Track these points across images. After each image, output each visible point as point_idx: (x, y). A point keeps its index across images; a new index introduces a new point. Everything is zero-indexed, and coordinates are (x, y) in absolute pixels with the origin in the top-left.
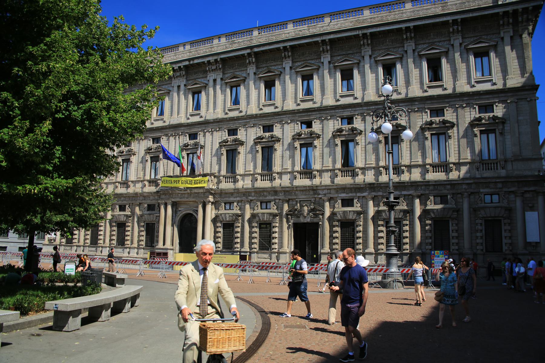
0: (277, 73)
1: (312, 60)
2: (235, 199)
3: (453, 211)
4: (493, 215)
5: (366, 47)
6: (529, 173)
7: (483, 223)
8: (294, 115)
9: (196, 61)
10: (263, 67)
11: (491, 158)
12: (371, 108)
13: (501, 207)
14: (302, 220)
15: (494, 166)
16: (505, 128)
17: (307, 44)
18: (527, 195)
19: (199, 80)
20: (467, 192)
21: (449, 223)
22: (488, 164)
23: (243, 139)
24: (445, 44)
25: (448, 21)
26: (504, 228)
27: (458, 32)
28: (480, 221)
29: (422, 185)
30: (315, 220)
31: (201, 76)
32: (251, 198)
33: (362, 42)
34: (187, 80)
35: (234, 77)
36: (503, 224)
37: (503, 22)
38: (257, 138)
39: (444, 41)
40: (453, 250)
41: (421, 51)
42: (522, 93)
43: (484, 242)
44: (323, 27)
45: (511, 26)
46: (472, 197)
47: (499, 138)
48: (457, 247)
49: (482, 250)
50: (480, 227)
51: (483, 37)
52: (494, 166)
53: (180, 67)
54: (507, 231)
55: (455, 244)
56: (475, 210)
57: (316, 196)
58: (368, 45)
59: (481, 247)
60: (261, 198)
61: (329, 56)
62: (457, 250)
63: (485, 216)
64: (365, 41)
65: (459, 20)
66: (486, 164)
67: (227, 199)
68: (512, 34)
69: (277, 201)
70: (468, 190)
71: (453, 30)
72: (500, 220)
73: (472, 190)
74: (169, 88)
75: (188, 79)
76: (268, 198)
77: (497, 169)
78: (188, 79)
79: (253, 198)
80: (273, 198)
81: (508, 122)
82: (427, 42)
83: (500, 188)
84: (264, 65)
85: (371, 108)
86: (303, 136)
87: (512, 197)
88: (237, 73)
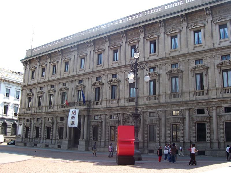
2: (99, 114)
4: (229, 120)
12: (164, 61)
17: (133, 29)
20: (215, 106)
21: (205, 125)
22: (227, 89)
23: (104, 82)
24: (203, 21)
27: (209, 14)
32: (106, 113)
35: (99, 50)
38: (109, 81)
40: (207, 140)
41: (190, 27)
46: (218, 109)
50: (222, 127)
51: (224, 16)
58: (163, 26)
60: (111, 113)
63: (225, 120)
65: (209, 8)
67: (95, 114)
69: (119, 114)
70: (215, 105)
71: (207, 13)
73: (217, 105)
76: (114, 113)
79: (107, 113)
82: (194, 21)
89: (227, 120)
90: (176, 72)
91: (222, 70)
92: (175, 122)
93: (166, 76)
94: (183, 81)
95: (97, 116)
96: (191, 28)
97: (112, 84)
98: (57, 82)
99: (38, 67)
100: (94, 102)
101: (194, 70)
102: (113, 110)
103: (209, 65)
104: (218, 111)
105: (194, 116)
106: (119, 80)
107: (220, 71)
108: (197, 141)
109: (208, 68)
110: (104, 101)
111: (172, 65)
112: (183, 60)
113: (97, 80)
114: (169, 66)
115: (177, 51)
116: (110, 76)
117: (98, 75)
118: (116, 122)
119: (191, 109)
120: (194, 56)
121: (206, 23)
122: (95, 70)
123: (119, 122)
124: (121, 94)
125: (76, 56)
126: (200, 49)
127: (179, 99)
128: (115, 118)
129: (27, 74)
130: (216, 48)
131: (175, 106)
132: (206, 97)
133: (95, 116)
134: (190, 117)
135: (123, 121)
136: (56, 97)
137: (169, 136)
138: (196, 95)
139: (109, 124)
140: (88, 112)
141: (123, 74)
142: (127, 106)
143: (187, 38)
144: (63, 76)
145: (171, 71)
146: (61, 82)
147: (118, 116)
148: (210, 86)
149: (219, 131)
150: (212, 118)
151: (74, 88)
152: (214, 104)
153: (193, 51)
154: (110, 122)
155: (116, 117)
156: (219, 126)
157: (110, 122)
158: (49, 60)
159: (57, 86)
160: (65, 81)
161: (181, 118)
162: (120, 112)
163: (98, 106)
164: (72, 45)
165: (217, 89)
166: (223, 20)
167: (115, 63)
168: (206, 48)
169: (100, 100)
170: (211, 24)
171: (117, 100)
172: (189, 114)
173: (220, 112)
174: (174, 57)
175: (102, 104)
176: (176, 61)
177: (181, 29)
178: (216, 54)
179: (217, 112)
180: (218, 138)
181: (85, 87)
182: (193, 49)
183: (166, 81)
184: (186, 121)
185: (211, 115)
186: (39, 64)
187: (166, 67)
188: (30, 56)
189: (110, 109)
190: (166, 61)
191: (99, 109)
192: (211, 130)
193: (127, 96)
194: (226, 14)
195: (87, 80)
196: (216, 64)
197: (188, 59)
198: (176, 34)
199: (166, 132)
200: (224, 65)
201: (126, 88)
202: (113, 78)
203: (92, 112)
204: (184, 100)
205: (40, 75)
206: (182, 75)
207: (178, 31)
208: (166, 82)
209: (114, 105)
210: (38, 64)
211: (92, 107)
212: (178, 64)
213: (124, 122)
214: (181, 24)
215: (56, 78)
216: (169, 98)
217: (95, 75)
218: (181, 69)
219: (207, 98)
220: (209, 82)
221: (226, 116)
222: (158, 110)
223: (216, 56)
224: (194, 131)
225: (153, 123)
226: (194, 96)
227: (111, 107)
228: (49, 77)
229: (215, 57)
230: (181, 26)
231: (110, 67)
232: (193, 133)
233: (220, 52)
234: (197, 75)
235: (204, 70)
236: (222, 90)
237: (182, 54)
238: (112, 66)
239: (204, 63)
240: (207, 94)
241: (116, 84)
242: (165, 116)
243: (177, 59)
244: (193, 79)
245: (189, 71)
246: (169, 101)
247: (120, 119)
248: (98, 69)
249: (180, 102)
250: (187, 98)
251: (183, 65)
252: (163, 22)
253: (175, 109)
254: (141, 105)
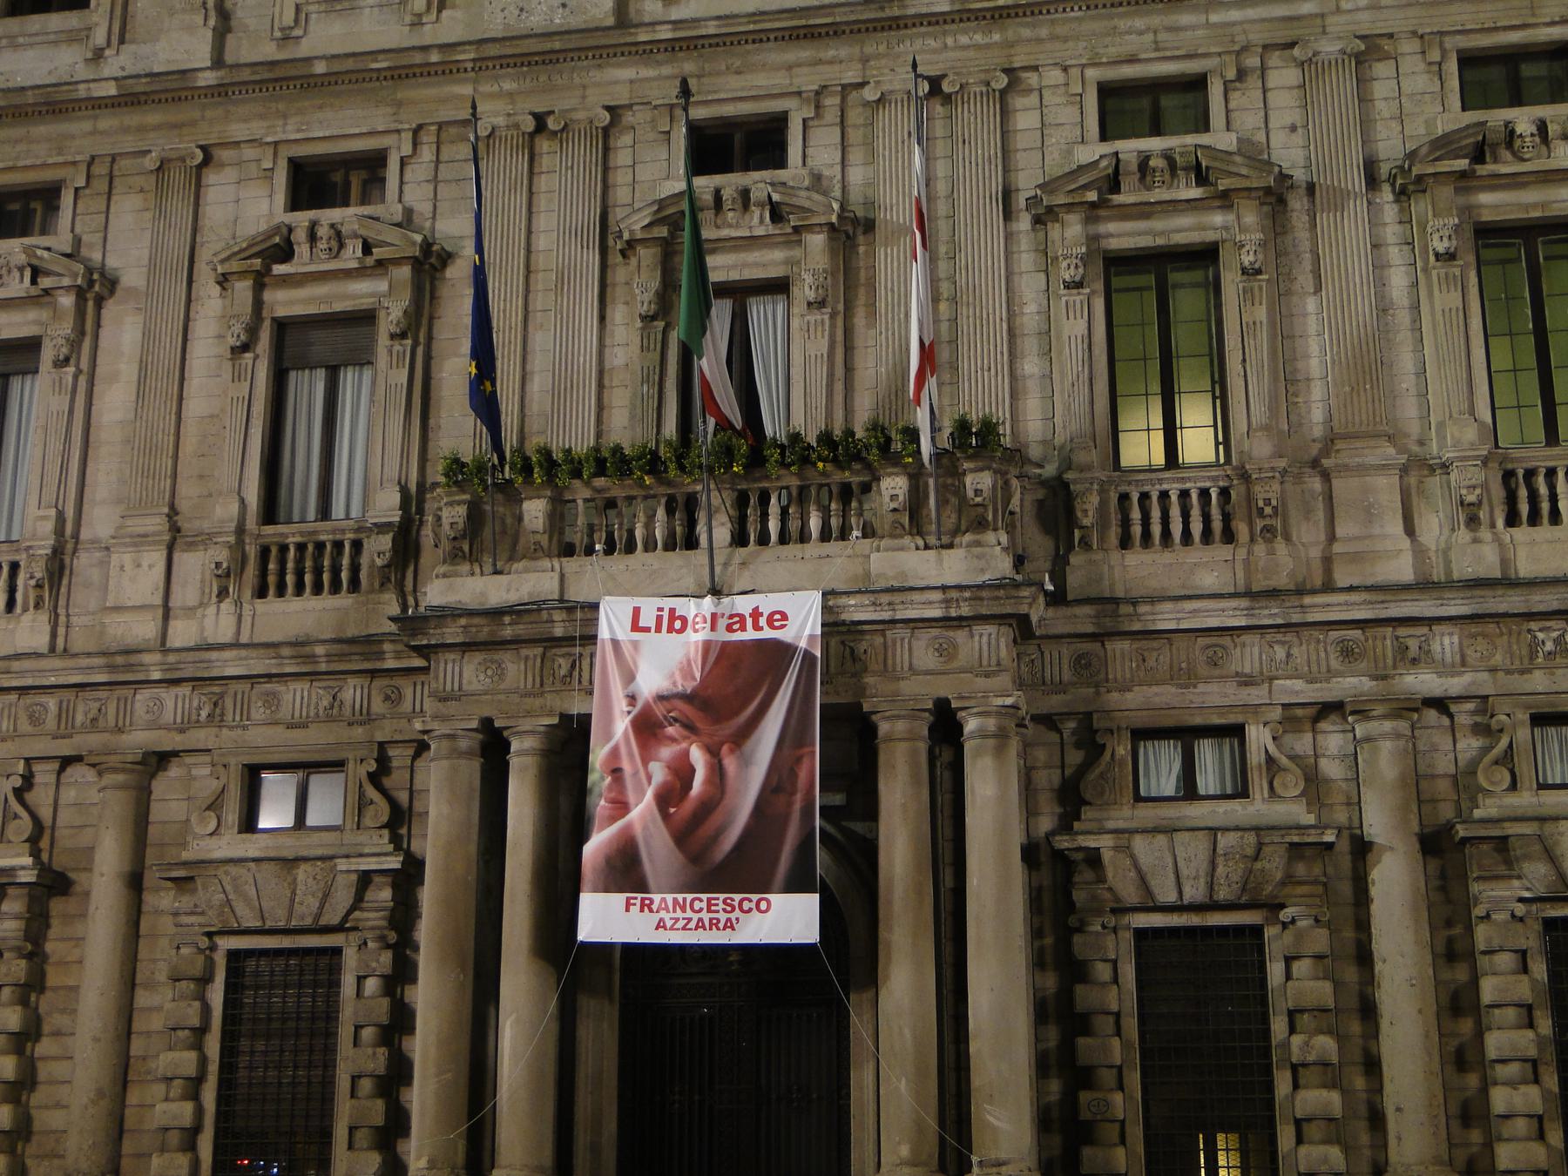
32: (1422, 682)
60: (1538, 681)
79: (1454, 685)
98: (157, 136)
146: (238, 131)
159: (129, 212)
191: (1270, 614)
217: (1075, 52)
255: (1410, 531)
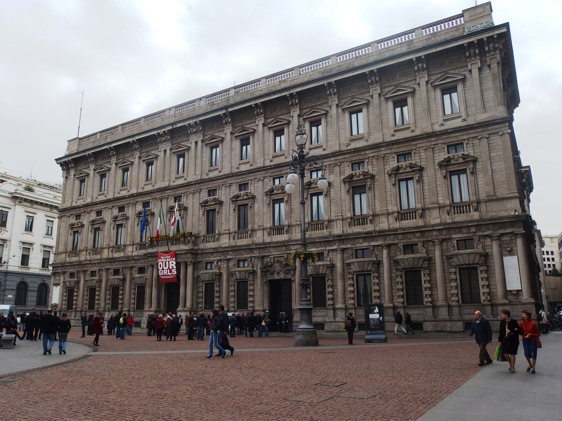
0: (251, 131)
1: (283, 115)
2: (215, 259)
3: (424, 260)
4: (467, 262)
5: (332, 96)
6: (505, 214)
7: (458, 272)
8: (267, 172)
9: (178, 125)
10: (239, 126)
11: (464, 200)
12: (339, 158)
13: (475, 254)
14: (276, 277)
15: (466, 209)
16: (477, 167)
18: (505, 238)
19: (183, 143)
23: (223, 199)
24: (412, 84)
25: (412, 59)
26: (480, 276)
27: (423, 69)
28: (454, 270)
29: (390, 235)
30: (289, 277)
31: (184, 139)
32: (229, 257)
33: (328, 92)
34: (172, 144)
36: (479, 272)
37: (470, 54)
38: (233, 197)
39: (410, 81)
41: (386, 94)
42: (493, 127)
43: (460, 293)
44: (293, 80)
45: (478, 57)
46: (444, 244)
47: (471, 178)
48: (430, 299)
49: (458, 301)
50: (453, 277)
52: (466, 209)
53: (164, 132)
54: (484, 279)
55: (428, 296)
56: (449, 258)
57: (288, 252)
58: (335, 94)
59: (456, 298)
60: (238, 256)
61: (298, 109)
62: (431, 302)
64: (331, 90)
66: (457, 207)
67: (208, 259)
68: (479, 66)
69: (253, 259)
71: (418, 68)
72: (477, 267)
73: (443, 237)
74: (157, 153)
75: (173, 143)
76: (244, 256)
77: (470, 212)
78: (173, 143)
79: (231, 257)
80: (248, 256)
81: (480, 160)
83: (473, 233)
84: (240, 124)
85: (339, 158)
86: (275, 191)
87: (488, 241)
88: (216, 134)
89: (462, 263)
90: (361, 177)
91: (450, 172)
92: (362, 269)
93: (343, 185)
94: (374, 194)
95: (212, 263)
96: (388, 96)
97: (239, 203)
98: (132, 201)
99: (91, 173)
100: (204, 236)
101: (395, 172)
102: (242, 252)
103: (423, 164)
104: (444, 247)
105: (399, 257)
106: (253, 196)
107: (446, 173)
108: (406, 304)
109: (423, 168)
110: (226, 234)
111: (352, 164)
112: (374, 154)
113: (209, 195)
114: (348, 168)
115: (361, 138)
116: (235, 188)
117: (211, 185)
118: (250, 273)
119: (393, 244)
120: (396, 146)
121: (416, 87)
122: (206, 177)
123: (254, 273)
124: (256, 220)
125: (168, 151)
126: (407, 134)
127: (369, 227)
128: (246, 265)
129: (69, 186)
130: (437, 132)
131: (361, 241)
132: (420, 222)
133: (207, 263)
134: (390, 260)
135: (262, 272)
136: (129, 229)
137: (352, 295)
138: (400, 218)
139: (235, 276)
140: (194, 256)
141: (260, 183)
142: (269, 243)
143: (381, 114)
144: (143, 188)
145: (351, 177)
146: (138, 200)
147: (252, 262)
148: (427, 200)
149: (448, 285)
150: (433, 261)
151: (165, 212)
152: (436, 235)
153: (393, 139)
154: (237, 273)
155: (249, 264)
156: (446, 275)
157: (237, 273)
158: (114, 160)
159: (130, 208)
160: (146, 198)
161: (374, 263)
162: (256, 254)
163: (212, 245)
164: (159, 131)
165: (440, 207)
166: (450, 80)
167: (245, 163)
168: (418, 132)
169: (217, 232)
170: (427, 88)
171: (249, 232)
172: (389, 254)
173: (448, 249)
174: (357, 150)
175: (221, 240)
176: (361, 157)
177: (369, 98)
178: (436, 142)
179: (442, 249)
180: (447, 298)
181: (186, 209)
182: (393, 135)
183: (342, 194)
184: (383, 266)
185: (431, 255)
186: (93, 168)
187: (342, 169)
188: (75, 152)
189: (236, 249)
190: (341, 157)
192: (433, 282)
193: (269, 225)
194: (455, 69)
195: (191, 196)
196: (437, 161)
197: (384, 152)
198: (360, 107)
199: (346, 290)
200: (453, 162)
201: (266, 208)
202: (240, 190)
203: (202, 256)
204: (377, 229)
205: (97, 188)
206: (374, 182)
207: (364, 102)
208: (342, 197)
209: (244, 242)
210: (92, 167)
211: (202, 246)
212: (364, 162)
213: (264, 273)
214: (368, 88)
215: (130, 193)
216: (350, 226)
217: (206, 187)
218: (371, 172)
219: (423, 224)
220: (425, 194)
221: (460, 257)
222: (328, 248)
223: (437, 146)
224: (400, 286)
225: (320, 272)
226: (396, 221)
227: (238, 244)
228: (114, 192)
229: (435, 149)
230: (369, 92)
231: (235, 171)
232: (398, 289)
233: (445, 138)
234: (401, 183)
235: (414, 173)
236: (450, 209)
237: (372, 145)
238: (238, 168)
239: (415, 160)
240: (422, 216)
241: (246, 202)
242: (343, 259)
243: (363, 153)
244: (395, 190)
245: (387, 176)
246: (349, 232)
247: (257, 267)
248: (212, 175)
249: (370, 233)
250: (384, 224)
251: (374, 163)
252: (334, 86)
253: (361, 245)
254: (296, 241)
255: (230, 240)
